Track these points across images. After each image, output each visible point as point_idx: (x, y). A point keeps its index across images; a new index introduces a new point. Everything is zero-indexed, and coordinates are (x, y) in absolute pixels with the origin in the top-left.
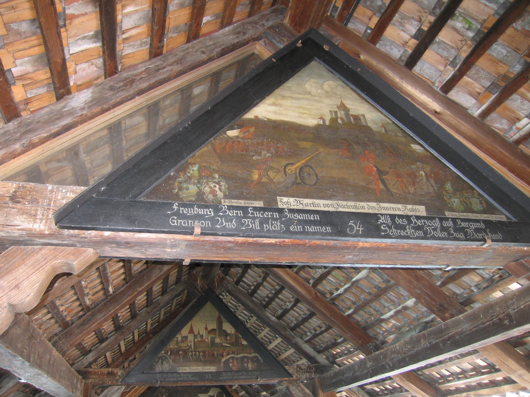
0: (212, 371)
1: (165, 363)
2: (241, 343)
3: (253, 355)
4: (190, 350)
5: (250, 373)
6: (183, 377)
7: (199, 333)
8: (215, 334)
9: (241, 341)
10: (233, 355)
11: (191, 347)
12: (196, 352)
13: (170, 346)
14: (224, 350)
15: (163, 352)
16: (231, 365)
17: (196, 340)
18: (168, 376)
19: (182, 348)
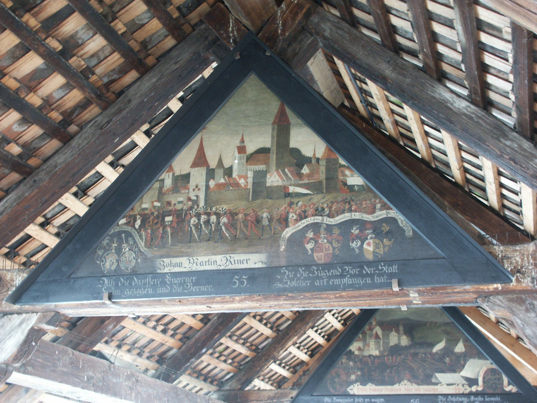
0: (253, 266)
1: (126, 248)
2: (345, 184)
3: (381, 214)
4: (193, 212)
5: (367, 270)
7: (220, 163)
8: (266, 162)
9: (344, 175)
10: (318, 219)
11: (196, 202)
12: (209, 214)
13: (142, 203)
14: (291, 204)
15: (123, 221)
16: (309, 246)
17: (212, 183)
18: (130, 284)
19: (170, 208)
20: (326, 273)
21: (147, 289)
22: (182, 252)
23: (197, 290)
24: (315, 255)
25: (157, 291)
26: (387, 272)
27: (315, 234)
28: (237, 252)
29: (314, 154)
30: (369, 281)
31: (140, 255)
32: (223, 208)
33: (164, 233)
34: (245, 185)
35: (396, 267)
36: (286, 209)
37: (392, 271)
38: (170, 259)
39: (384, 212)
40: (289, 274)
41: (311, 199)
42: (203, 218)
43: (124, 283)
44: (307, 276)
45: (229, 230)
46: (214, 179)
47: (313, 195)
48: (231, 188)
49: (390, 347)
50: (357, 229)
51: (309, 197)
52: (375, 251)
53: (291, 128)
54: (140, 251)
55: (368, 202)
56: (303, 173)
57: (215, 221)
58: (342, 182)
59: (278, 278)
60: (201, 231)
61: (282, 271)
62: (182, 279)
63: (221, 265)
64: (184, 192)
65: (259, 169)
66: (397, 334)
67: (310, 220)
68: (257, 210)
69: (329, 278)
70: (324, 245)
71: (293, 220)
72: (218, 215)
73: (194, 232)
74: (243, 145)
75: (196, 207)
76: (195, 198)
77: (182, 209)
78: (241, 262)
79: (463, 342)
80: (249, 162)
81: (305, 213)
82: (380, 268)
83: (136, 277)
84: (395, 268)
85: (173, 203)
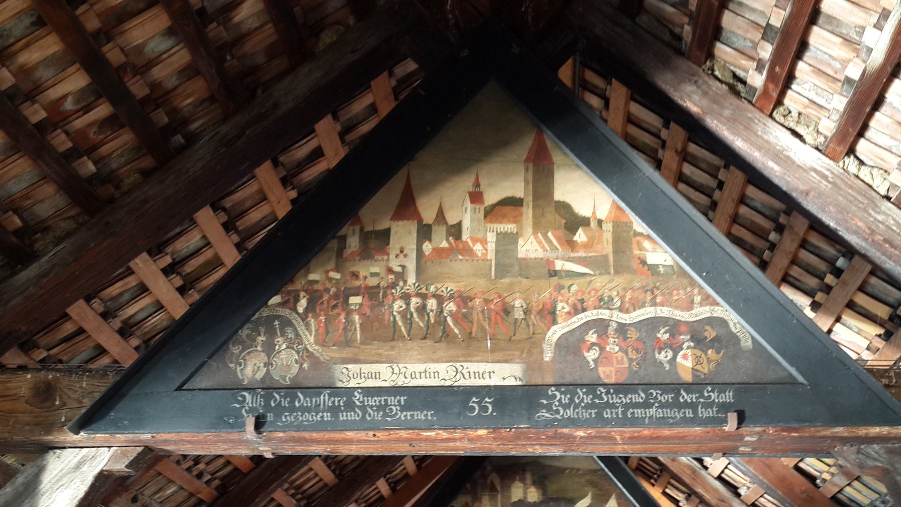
1: (281, 343)
2: (644, 262)
3: (701, 312)
4: (397, 292)
5: (685, 397)
6: (363, 408)
7: (441, 216)
8: (517, 220)
9: (641, 248)
10: (604, 314)
11: (401, 276)
12: (424, 297)
14: (559, 288)
15: (276, 300)
16: (591, 356)
17: (427, 247)
19: (358, 283)
20: (620, 398)
21: (321, 414)
22: (380, 354)
23: (409, 418)
24: (601, 370)
25: (339, 417)
26: (717, 401)
27: (599, 337)
28: (474, 359)
29: (594, 213)
30: (689, 414)
31: (307, 357)
32: (447, 288)
33: (349, 322)
34: (482, 254)
35: (731, 394)
36: (551, 295)
37: (724, 400)
38: (361, 366)
39: (707, 308)
40: (561, 398)
41: (591, 281)
42: (415, 301)
43: (281, 401)
44: (590, 402)
45: (459, 324)
46: (430, 240)
47: (595, 275)
48: (460, 257)
49: (512, 504)
50: (666, 332)
51: (588, 279)
52: (696, 368)
53: (555, 169)
54: (308, 351)
55: (681, 292)
56: (576, 241)
57: (435, 307)
58: (639, 258)
59: (542, 403)
60: (411, 323)
61: (550, 393)
62: (383, 399)
63: (447, 379)
64: (380, 258)
65: (506, 230)
66: (521, 485)
67: (591, 315)
68: (505, 295)
69: (626, 407)
70: (615, 355)
71: (563, 314)
72: (440, 299)
73: (400, 323)
74: (477, 190)
75: (401, 283)
76: (399, 269)
77: (378, 286)
78: (481, 376)
79: (617, 500)
80: (488, 218)
81: (582, 303)
82: (706, 395)
83: (302, 393)
84: (729, 395)
85: (362, 274)
